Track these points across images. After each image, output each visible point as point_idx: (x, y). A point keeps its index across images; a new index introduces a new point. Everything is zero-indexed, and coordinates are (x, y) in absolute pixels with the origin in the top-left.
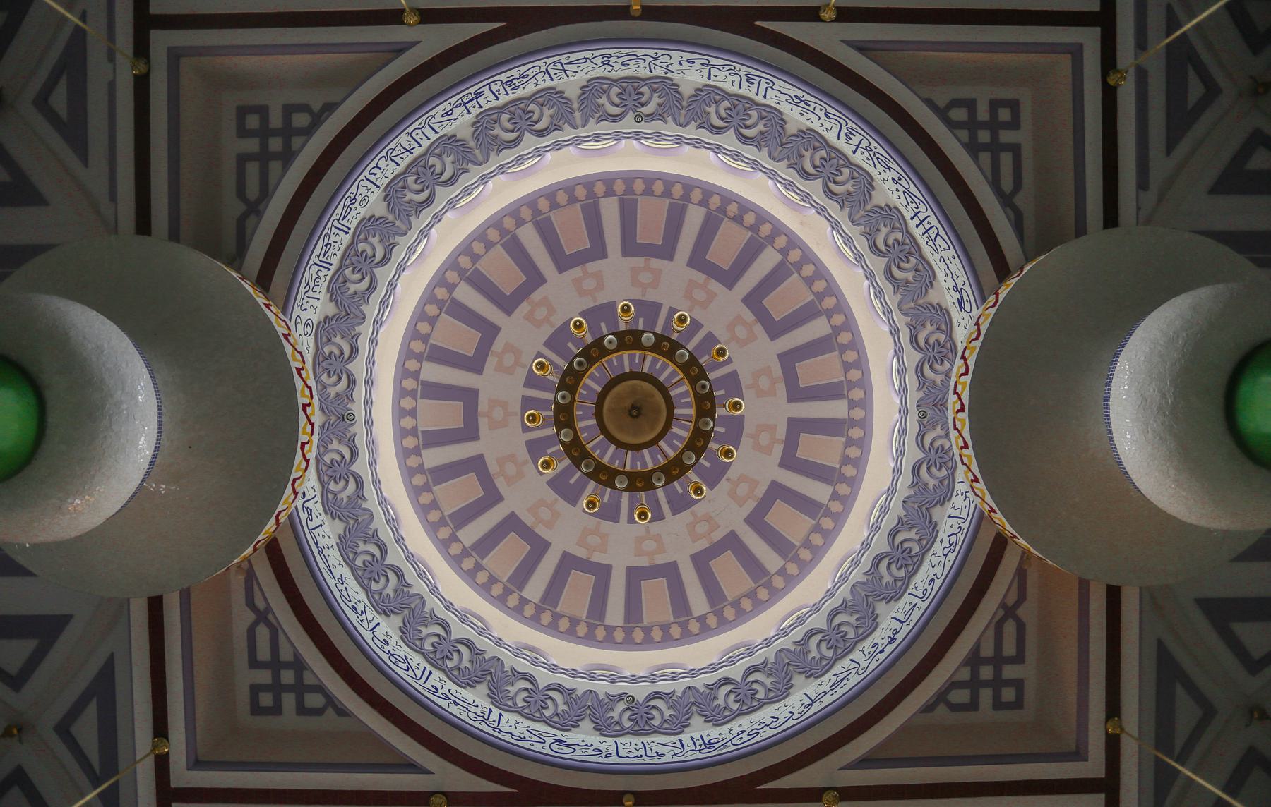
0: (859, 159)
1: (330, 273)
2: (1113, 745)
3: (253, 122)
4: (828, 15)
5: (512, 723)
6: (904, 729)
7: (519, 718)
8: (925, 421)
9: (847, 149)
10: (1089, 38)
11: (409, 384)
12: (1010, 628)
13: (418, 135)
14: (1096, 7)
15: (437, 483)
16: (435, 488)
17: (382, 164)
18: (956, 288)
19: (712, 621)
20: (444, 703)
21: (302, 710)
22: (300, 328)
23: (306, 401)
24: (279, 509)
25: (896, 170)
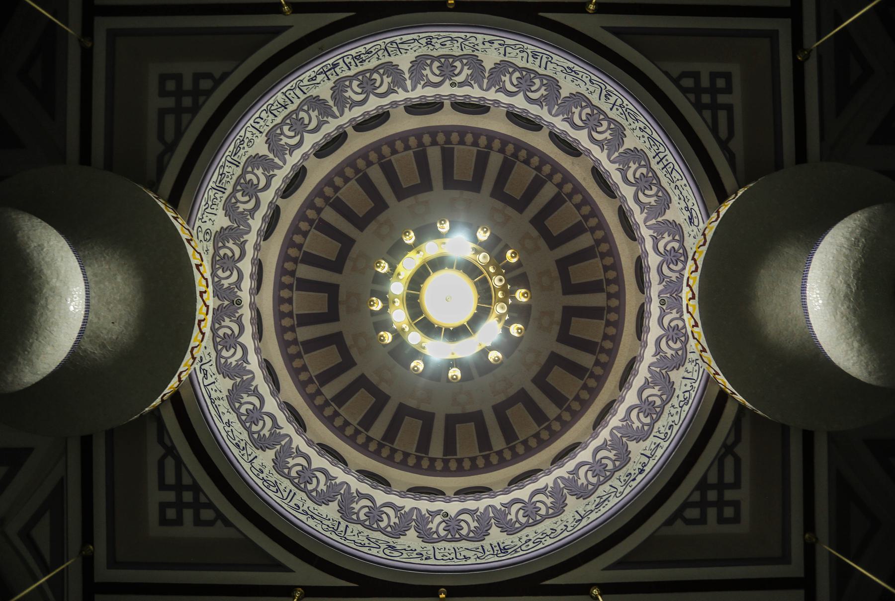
1: (225, 196)
2: (810, 550)
3: (171, 85)
5: (355, 532)
6: (651, 537)
7: (360, 528)
8: (664, 307)
9: (606, 107)
10: (783, 27)
11: (286, 279)
12: (729, 462)
13: (291, 94)
14: (788, 4)
16: (305, 356)
17: (264, 115)
18: (687, 209)
19: (508, 455)
20: (303, 518)
21: (198, 522)
22: (201, 235)
23: (203, 289)
24: (181, 370)
25: (644, 119)
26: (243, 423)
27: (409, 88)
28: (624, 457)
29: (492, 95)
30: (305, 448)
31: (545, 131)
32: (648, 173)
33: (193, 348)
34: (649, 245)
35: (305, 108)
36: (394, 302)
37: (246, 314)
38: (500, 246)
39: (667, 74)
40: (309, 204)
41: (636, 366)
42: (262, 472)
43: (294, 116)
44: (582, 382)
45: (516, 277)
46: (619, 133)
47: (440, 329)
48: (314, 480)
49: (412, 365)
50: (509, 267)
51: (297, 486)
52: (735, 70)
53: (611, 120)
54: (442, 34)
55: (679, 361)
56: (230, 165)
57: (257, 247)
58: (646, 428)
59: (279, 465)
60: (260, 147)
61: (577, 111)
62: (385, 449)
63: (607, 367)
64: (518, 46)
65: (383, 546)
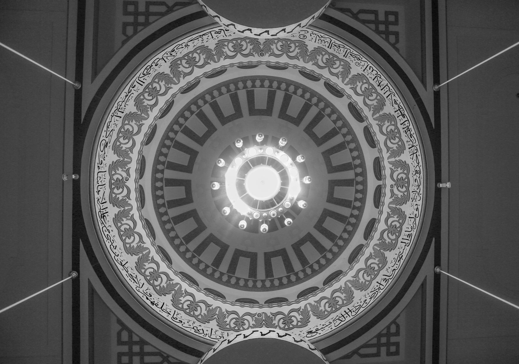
0: (374, 284)
1: (326, 48)
3: (392, 18)
4: (438, 270)
5: (116, 122)
7: (120, 125)
8: (256, 316)
9: (379, 278)
13: (386, 89)
15: (231, 96)
20: (126, 90)
22: (303, 33)
24: (221, 17)
26: (187, 55)
27: (390, 160)
28: (162, 292)
29: (386, 210)
30: (171, 92)
31: (364, 242)
32: (339, 305)
33: (234, 25)
34: (295, 306)
35: (378, 98)
36: (261, 149)
37: (255, 59)
38: (294, 214)
39: (399, 316)
40: (321, 99)
41: (220, 299)
42: (156, 65)
43: (373, 91)
44: (210, 264)
45: (275, 224)
46: (363, 287)
47: (244, 177)
48: (151, 98)
49: (222, 160)
50: (281, 220)
51: (147, 87)
52: (401, 357)
53: (371, 282)
54: (422, 180)
55: (222, 326)
56: (345, 51)
57: (295, 66)
58: (180, 306)
59: (161, 76)
60: (355, 70)
61: (376, 261)
62: (169, 142)
63: (219, 280)
64: (415, 225)
65: (107, 140)
